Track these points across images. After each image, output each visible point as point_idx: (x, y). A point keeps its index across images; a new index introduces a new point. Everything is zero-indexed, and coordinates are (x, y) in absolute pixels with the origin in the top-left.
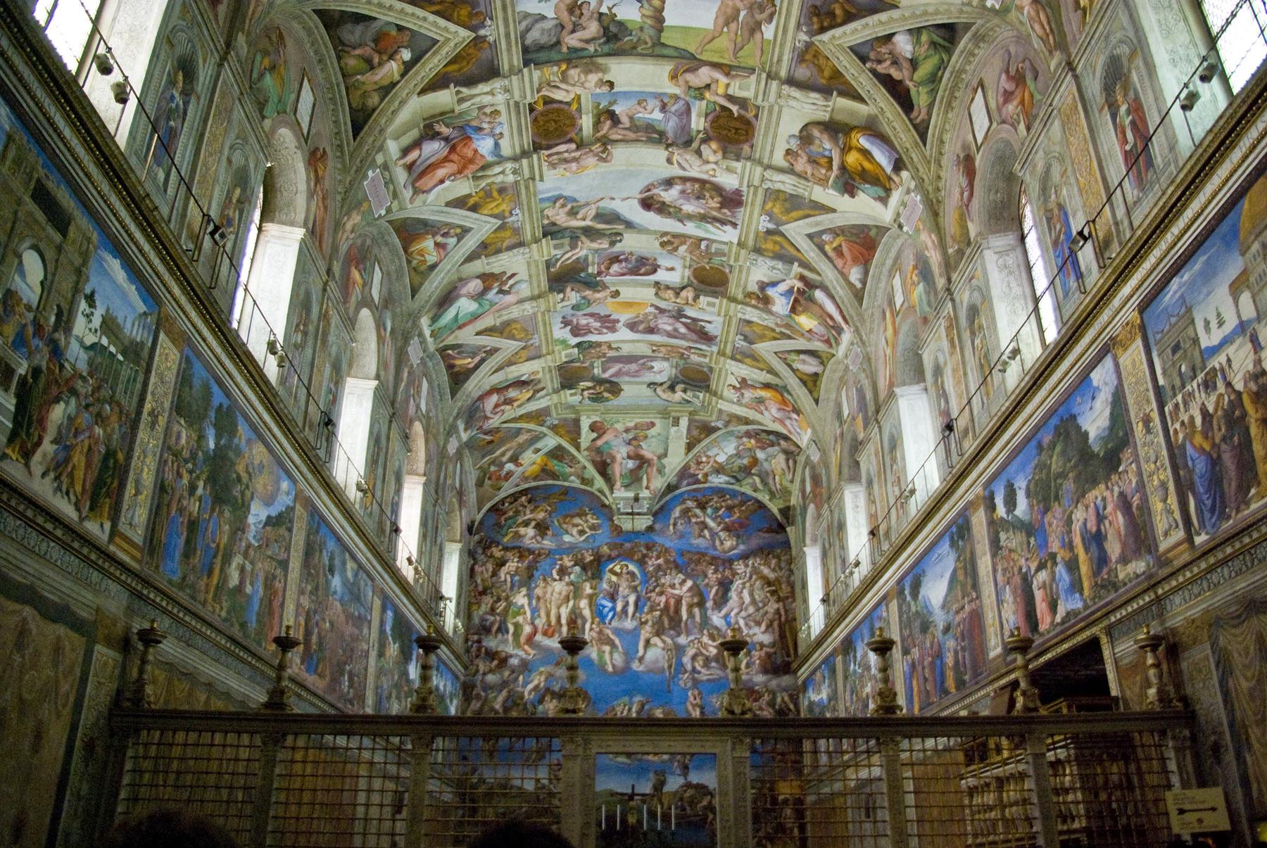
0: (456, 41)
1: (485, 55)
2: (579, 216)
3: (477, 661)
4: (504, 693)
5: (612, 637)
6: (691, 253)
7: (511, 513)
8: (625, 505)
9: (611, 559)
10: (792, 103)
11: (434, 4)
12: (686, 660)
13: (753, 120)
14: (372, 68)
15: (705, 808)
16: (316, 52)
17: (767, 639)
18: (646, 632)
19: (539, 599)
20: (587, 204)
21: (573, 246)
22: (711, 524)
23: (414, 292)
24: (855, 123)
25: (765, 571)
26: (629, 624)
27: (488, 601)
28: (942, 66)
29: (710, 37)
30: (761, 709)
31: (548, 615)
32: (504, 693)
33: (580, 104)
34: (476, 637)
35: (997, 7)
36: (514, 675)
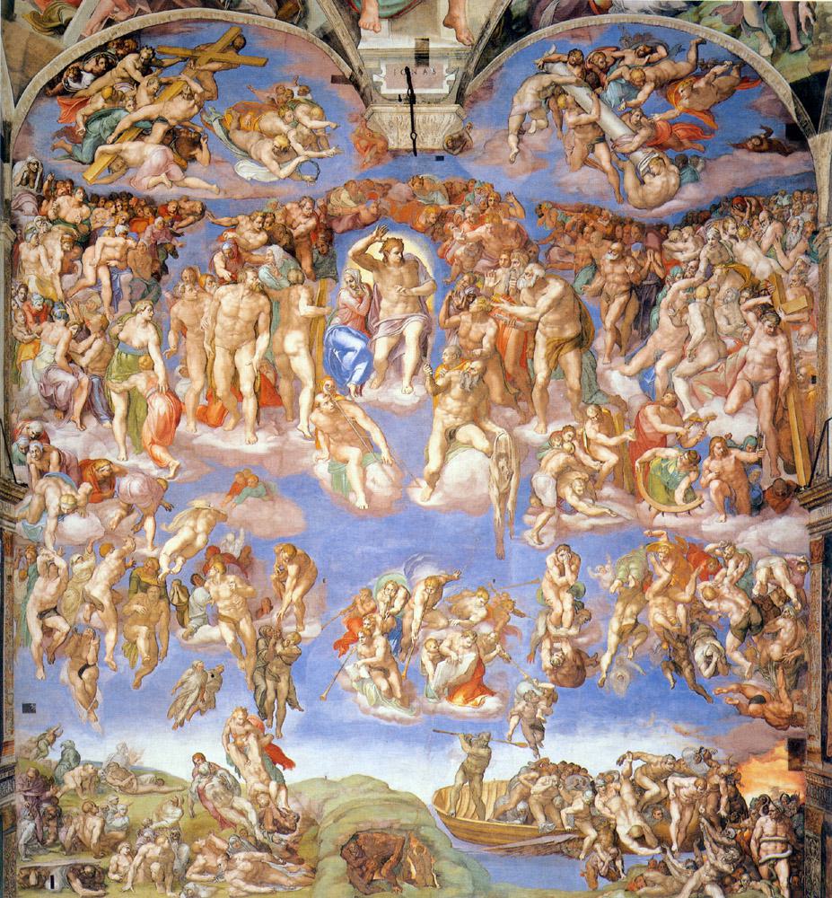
3: (40, 485)
4: (112, 560)
5: (366, 424)
7: (99, 103)
8: (392, 73)
9: (359, 226)
12: (543, 481)
15: (576, 815)
17: (742, 427)
18: (448, 410)
19: (183, 330)
22: (615, 127)
25: (749, 254)
26: (404, 393)
27: (57, 334)
30: (717, 596)
31: (207, 370)
32: (112, 560)
34: (35, 427)
36: (134, 517)
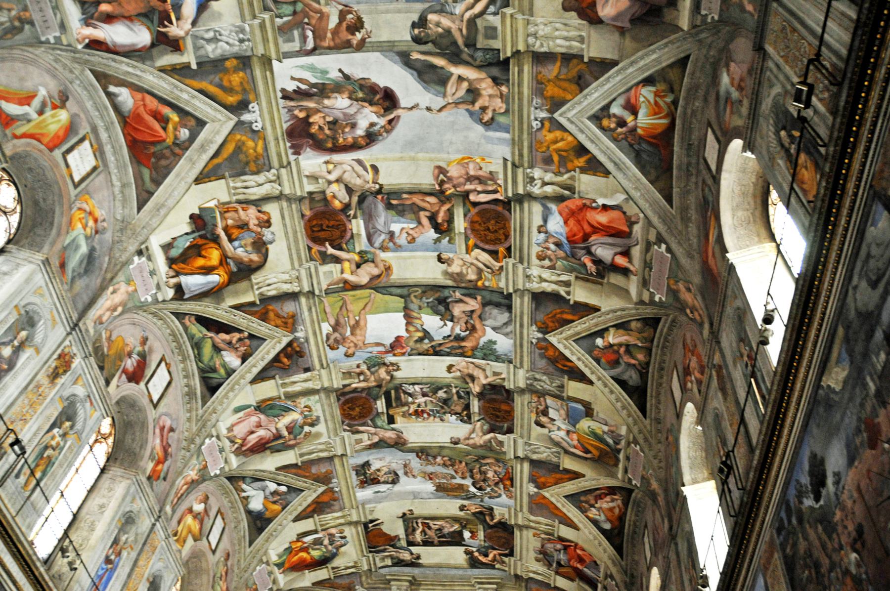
0: (560, 336)
1: (541, 317)
2: (465, 85)
6: (320, 12)
10: (286, 277)
11: (570, 367)
13: (311, 244)
14: (627, 346)
16: (661, 377)
20: (457, 104)
21: (472, 22)
23: (683, 62)
24: (231, 287)
28: (199, 357)
29: (367, 309)
33: (467, 245)
35: (203, 447)
